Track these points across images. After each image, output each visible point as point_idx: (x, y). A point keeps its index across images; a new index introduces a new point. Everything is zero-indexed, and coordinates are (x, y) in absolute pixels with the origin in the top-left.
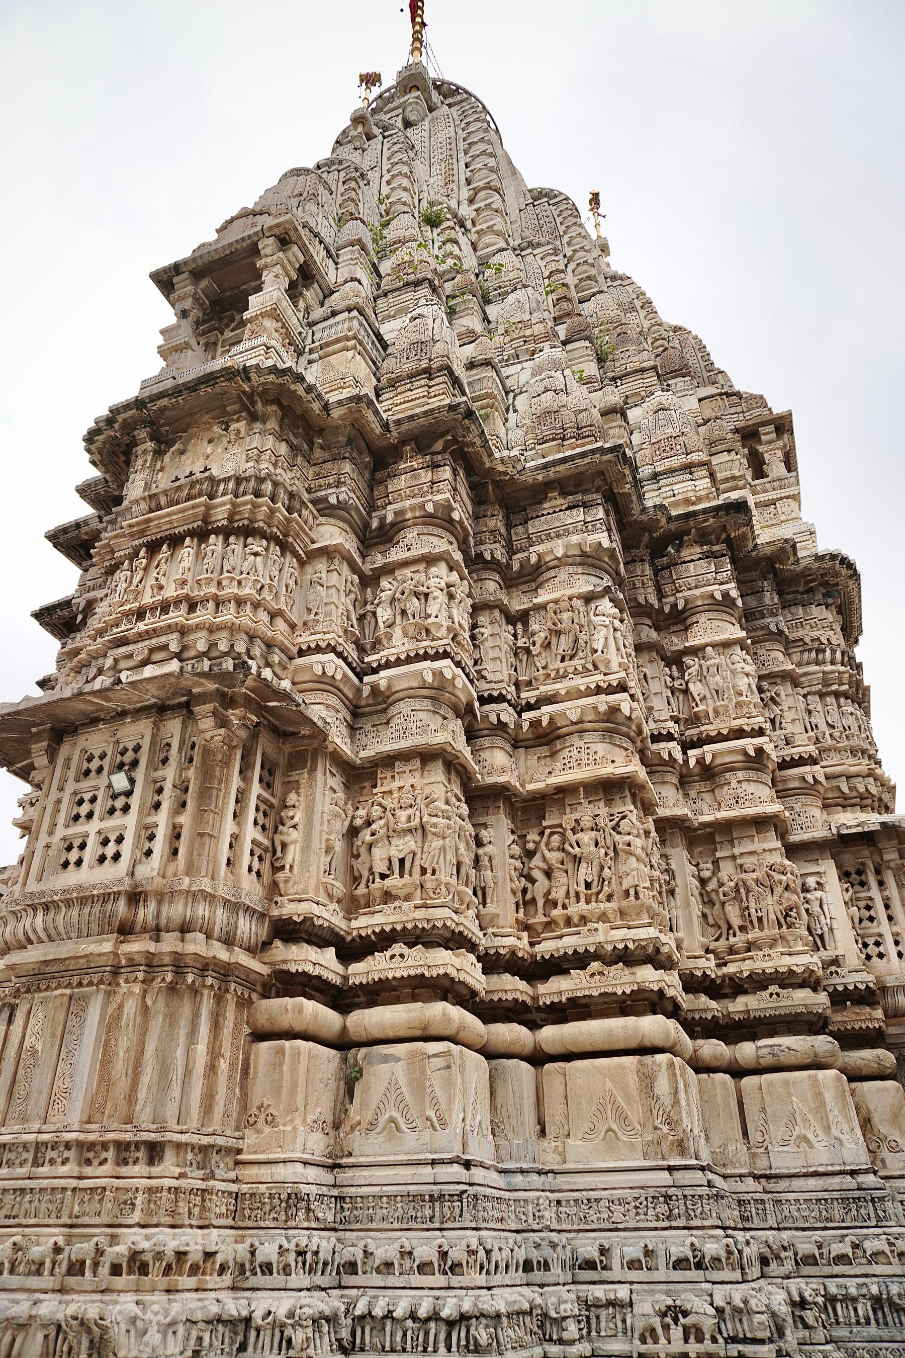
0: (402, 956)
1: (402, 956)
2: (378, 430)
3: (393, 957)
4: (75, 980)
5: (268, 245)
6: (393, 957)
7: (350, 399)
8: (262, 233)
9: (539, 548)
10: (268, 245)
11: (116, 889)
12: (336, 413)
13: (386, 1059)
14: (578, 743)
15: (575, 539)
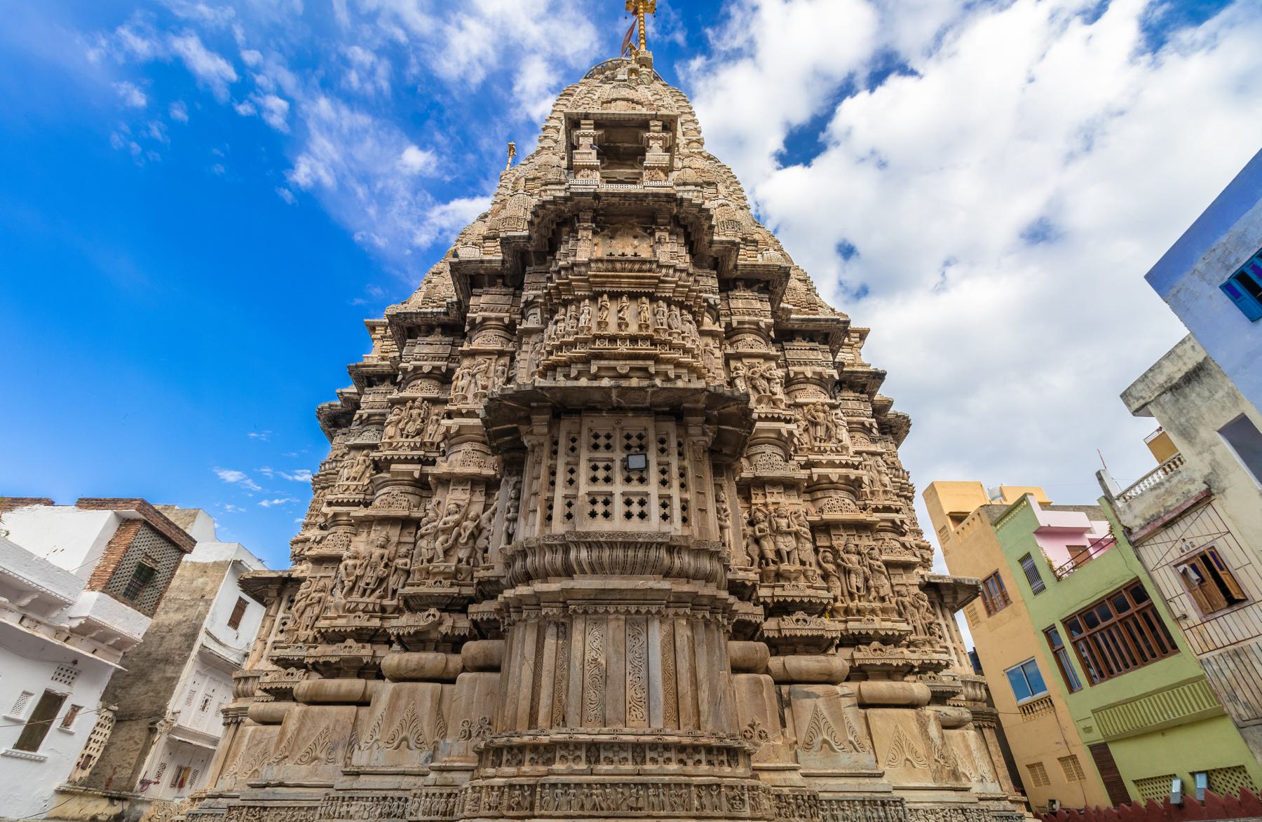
0: (805, 621)
1: (805, 621)
2: (731, 267)
3: (798, 620)
4: (633, 609)
5: (656, 125)
6: (798, 620)
7: (728, 242)
8: (656, 117)
9: (796, 369)
10: (656, 125)
11: (660, 540)
12: (715, 248)
13: (808, 695)
14: (835, 496)
15: (819, 369)
